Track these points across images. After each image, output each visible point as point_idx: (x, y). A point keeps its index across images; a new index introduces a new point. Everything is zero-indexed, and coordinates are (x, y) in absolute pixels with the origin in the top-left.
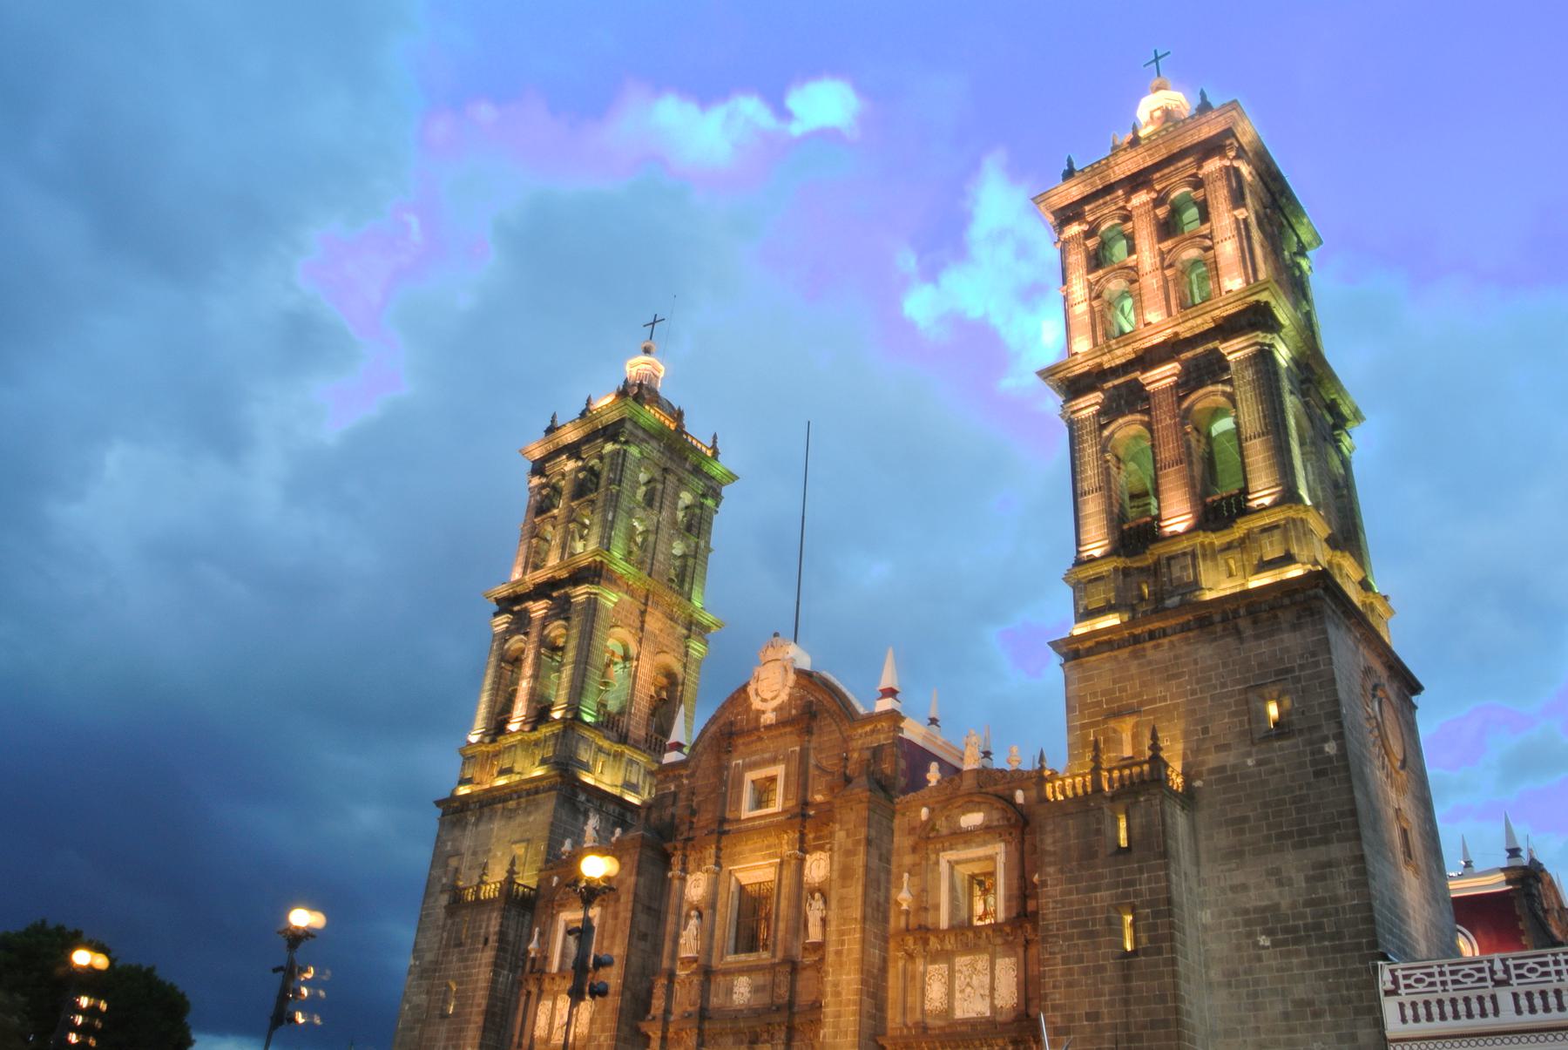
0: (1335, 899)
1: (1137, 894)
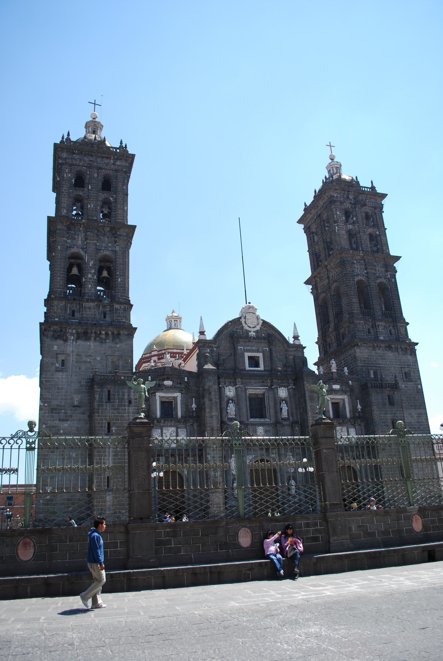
0: (422, 422)
1: (397, 417)
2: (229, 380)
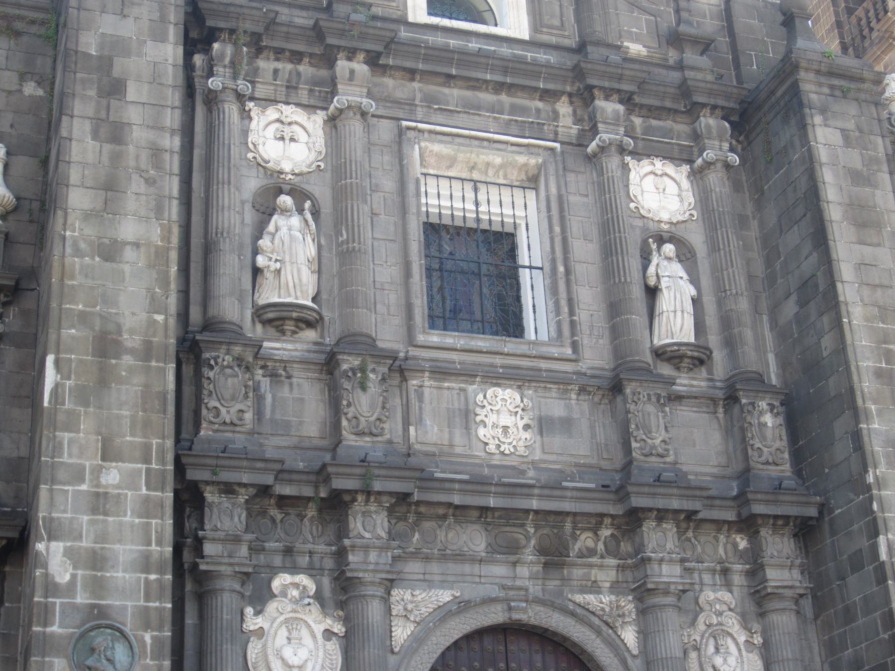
2: (286, 67)
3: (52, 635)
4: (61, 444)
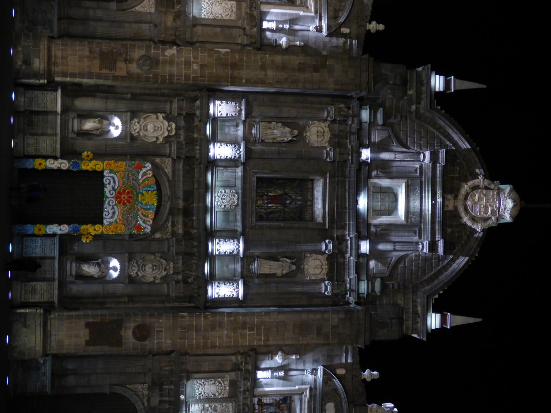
3: (151, 50)
4: (204, 53)
